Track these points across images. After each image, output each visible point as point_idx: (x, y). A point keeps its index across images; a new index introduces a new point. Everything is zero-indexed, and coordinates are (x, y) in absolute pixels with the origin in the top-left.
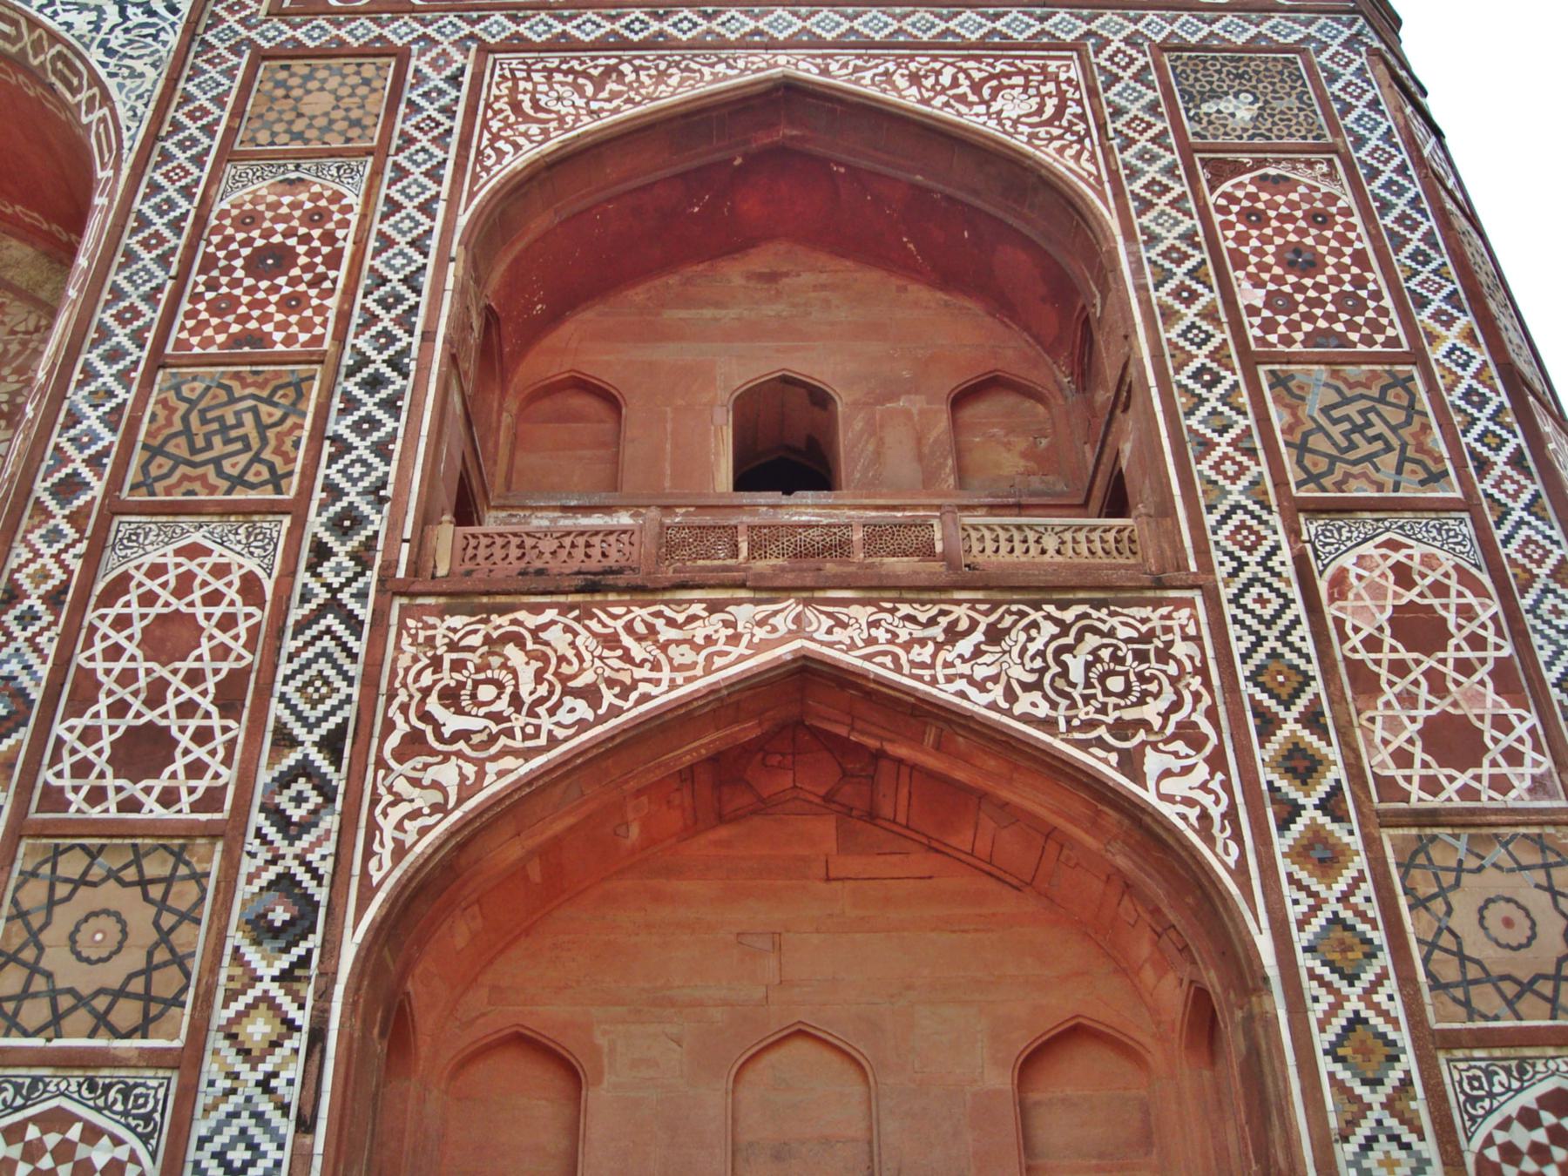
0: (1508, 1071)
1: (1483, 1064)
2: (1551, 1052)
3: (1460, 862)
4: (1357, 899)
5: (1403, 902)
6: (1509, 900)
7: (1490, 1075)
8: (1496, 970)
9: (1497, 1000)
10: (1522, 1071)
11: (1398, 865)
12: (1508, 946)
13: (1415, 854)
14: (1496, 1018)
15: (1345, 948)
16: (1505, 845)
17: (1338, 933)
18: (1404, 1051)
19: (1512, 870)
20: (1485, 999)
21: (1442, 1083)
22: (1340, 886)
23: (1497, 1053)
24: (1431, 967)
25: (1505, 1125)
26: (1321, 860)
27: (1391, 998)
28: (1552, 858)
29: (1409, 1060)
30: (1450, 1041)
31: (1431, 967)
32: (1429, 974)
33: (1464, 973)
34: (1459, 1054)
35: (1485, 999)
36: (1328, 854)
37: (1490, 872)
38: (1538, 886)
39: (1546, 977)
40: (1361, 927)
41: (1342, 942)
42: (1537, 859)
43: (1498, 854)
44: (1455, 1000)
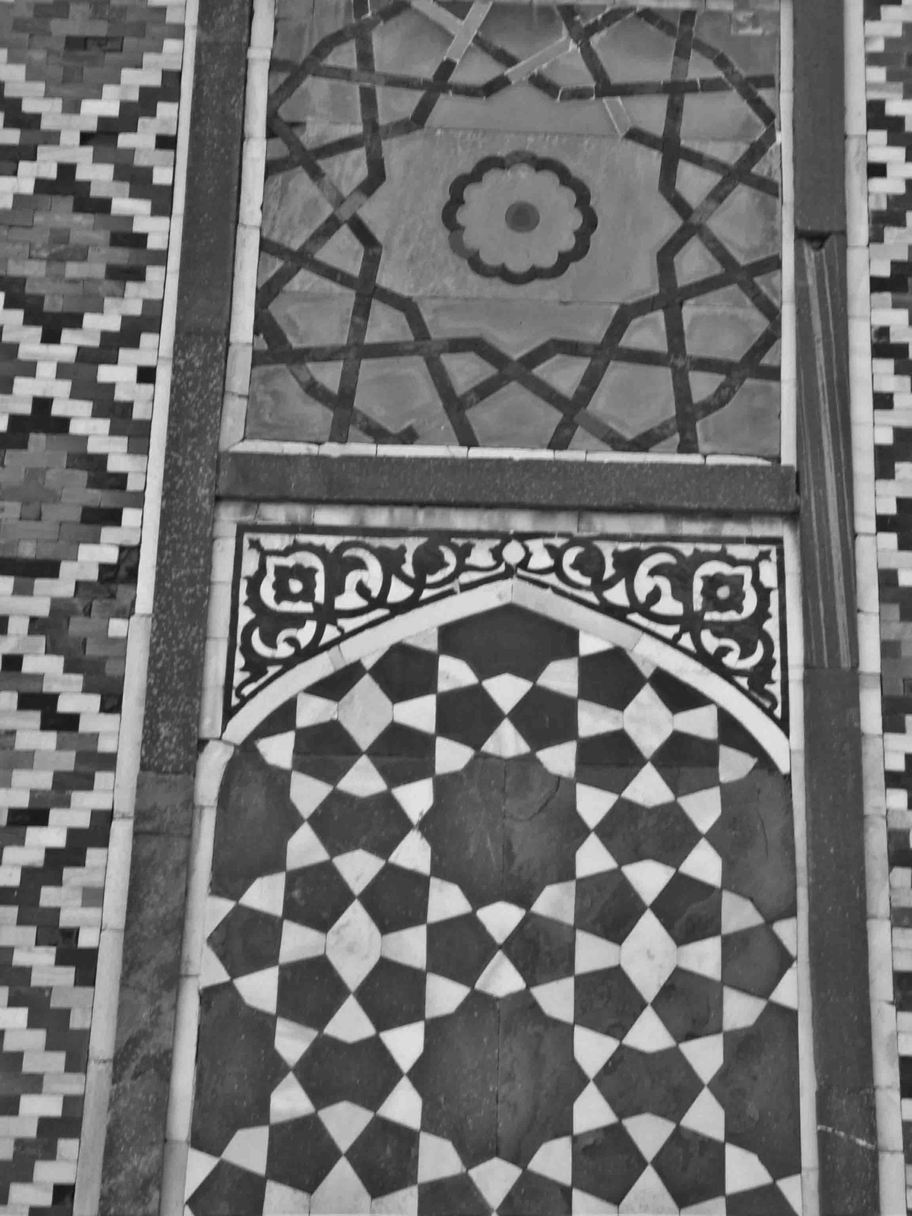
0: (391, 564)
1: (331, 542)
2: (521, 522)
3: (447, 67)
4: (139, 141)
5: (256, 153)
6: (541, 164)
7: (339, 566)
8: (443, 327)
9: (426, 395)
10: (428, 561)
11: (275, 65)
12: (504, 274)
13: (337, 39)
14: (409, 437)
15: (63, 249)
16: (583, 36)
17: (61, 214)
18: (138, 500)
19: (579, 94)
20: (395, 389)
21: (206, 579)
22: (108, 105)
23: (379, 518)
24: (276, 309)
25: (334, 687)
26: (75, 44)
27: (146, 375)
28: (699, 69)
29: (142, 525)
30: (256, 483)
31: (276, 309)
32: (264, 324)
33: (358, 330)
34: (277, 514)
35: (395, 389)
36: (101, 29)
37: (520, 99)
38: (636, 135)
39: (573, 349)
40: (123, 205)
41: (60, 237)
42: (660, 71)
43: (563, 56)
44: (313, 389)
